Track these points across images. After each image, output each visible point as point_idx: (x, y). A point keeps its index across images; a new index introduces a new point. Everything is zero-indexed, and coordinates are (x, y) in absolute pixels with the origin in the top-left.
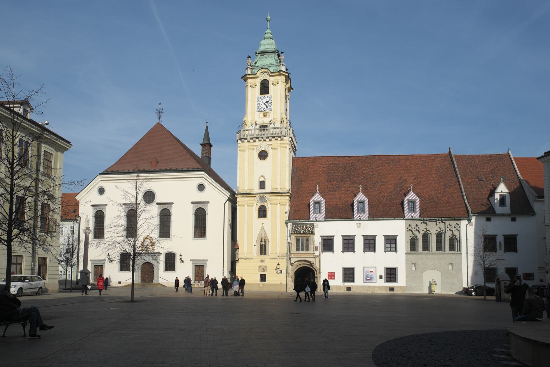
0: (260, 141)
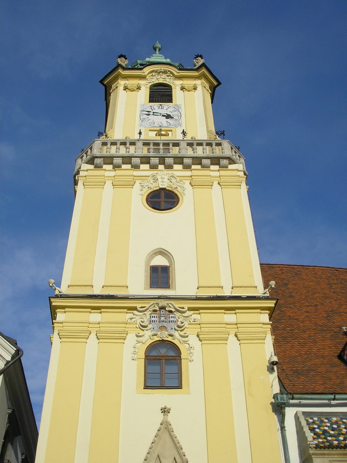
0: (154, 167)
